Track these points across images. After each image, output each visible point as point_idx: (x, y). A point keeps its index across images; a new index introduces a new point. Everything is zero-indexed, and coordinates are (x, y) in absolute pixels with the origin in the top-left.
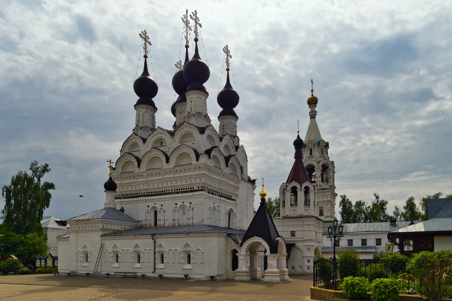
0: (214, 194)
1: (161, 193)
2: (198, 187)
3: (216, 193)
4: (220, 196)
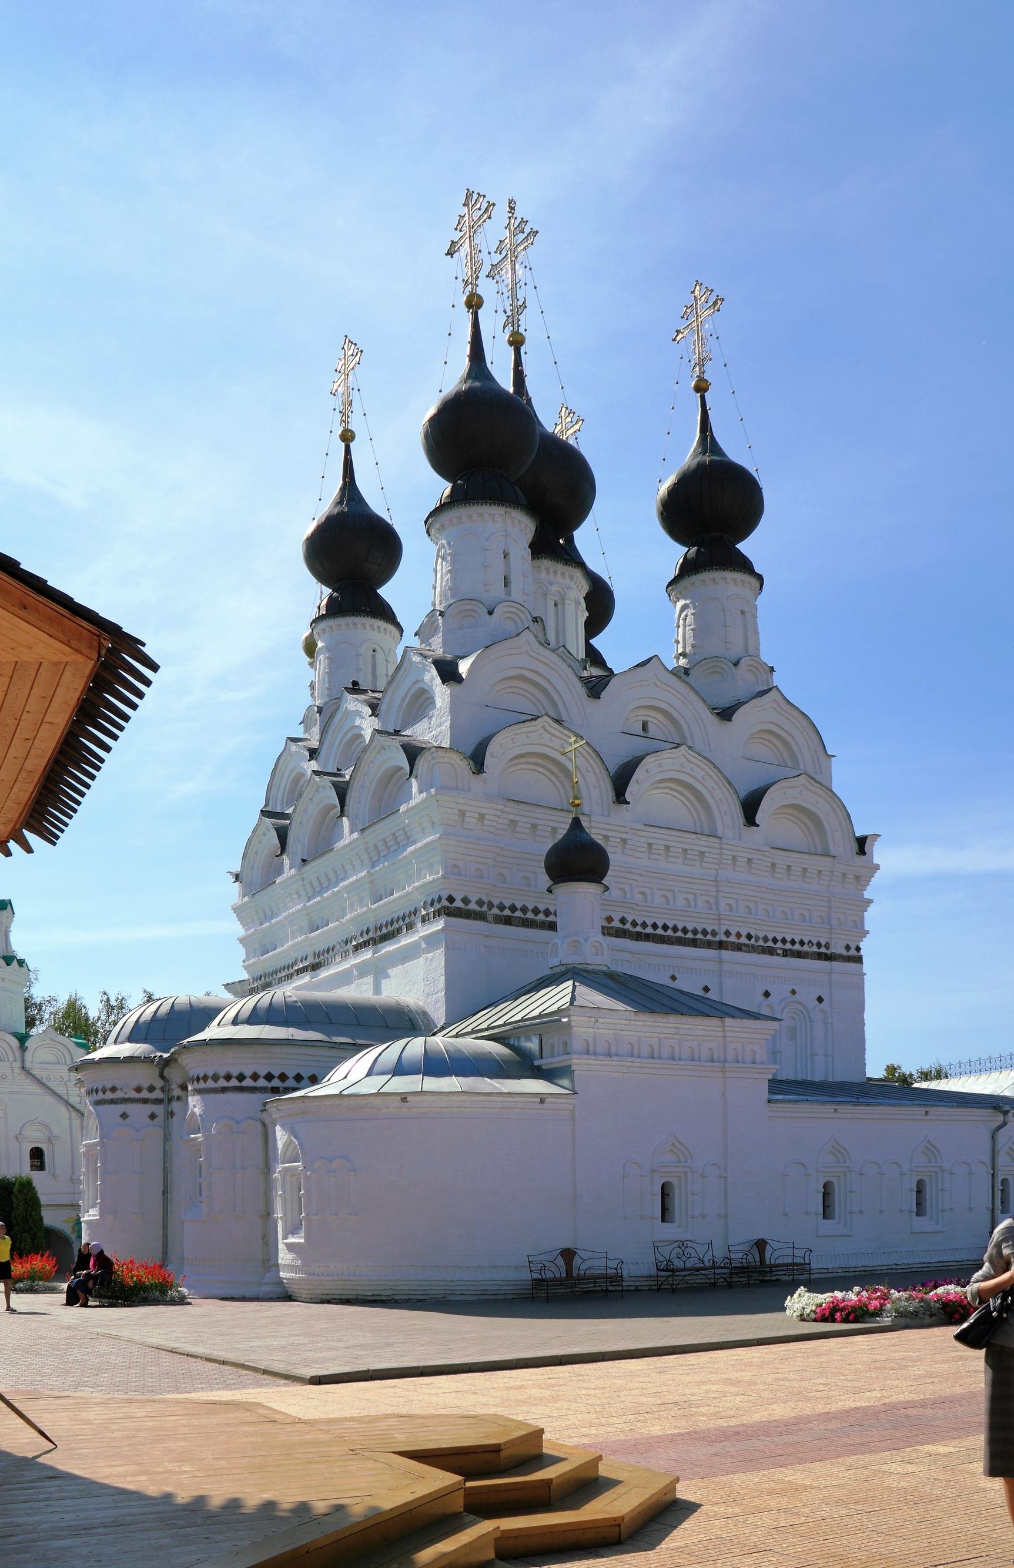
1: (699, 936)
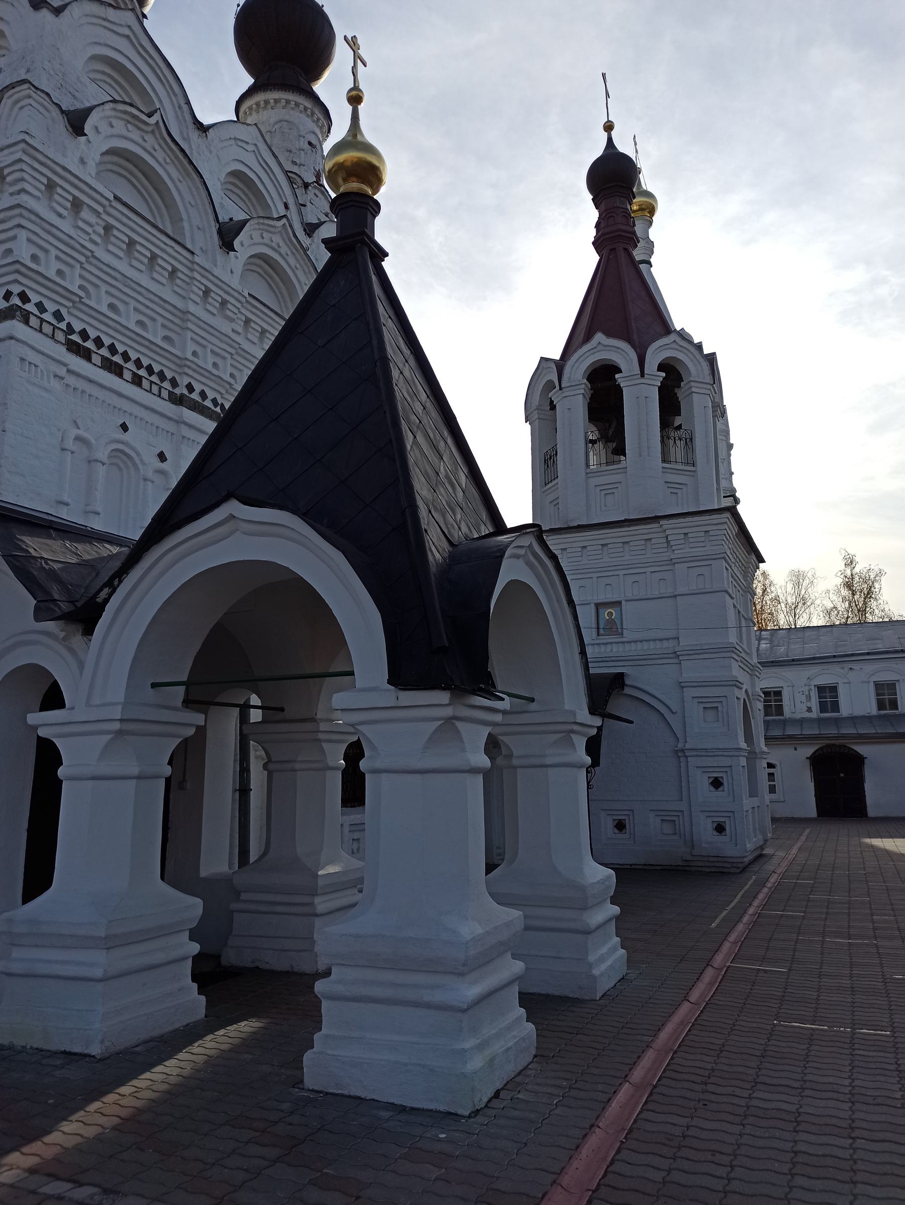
0: (127, 375)
3: (142, 372)
4: (178, 400)
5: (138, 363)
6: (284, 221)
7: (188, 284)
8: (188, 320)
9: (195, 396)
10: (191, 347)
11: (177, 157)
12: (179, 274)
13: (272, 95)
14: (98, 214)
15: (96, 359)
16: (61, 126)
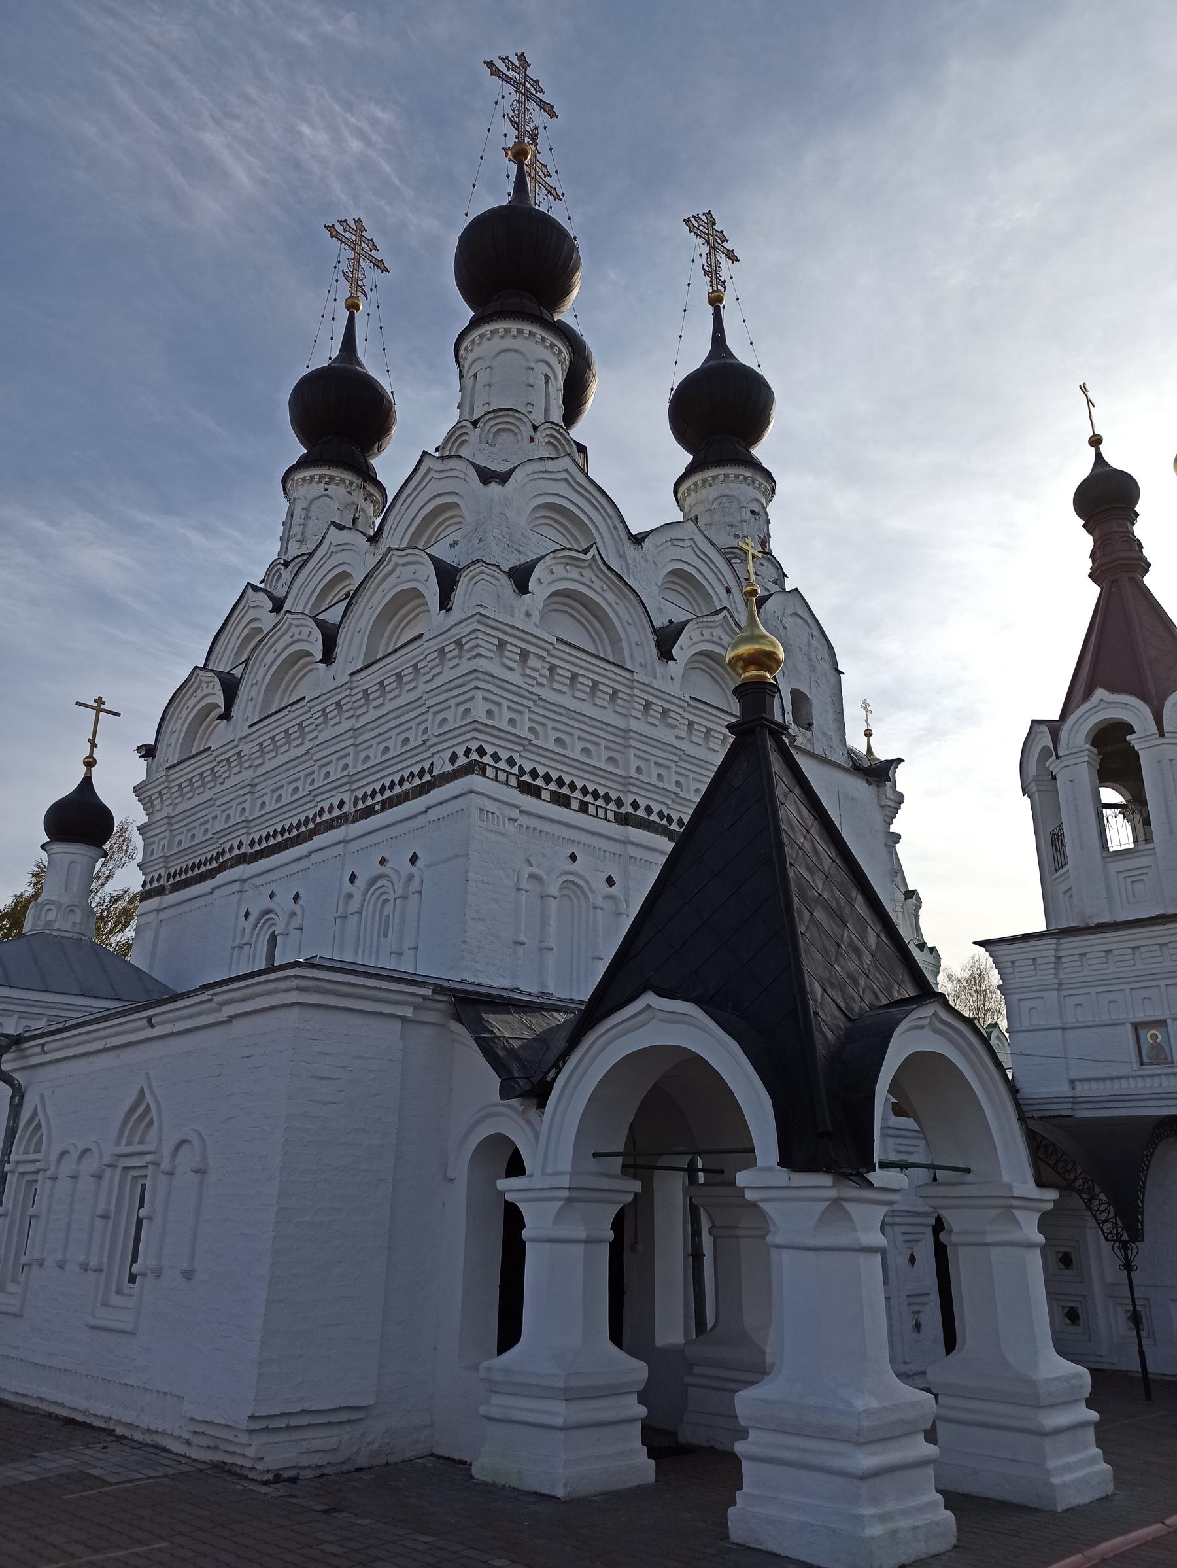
0: (575, 804)
2: (453, 758)
3: (589, 799)
4: (623, 820)
5: (584, 791)
6: (725, 612)
7: (628, 701)
8: (630, 738)
9: (641, 813)
10: (635, 763)
11: (613, 583)
12: (620, 695)
13: (709, 474)
14: (542, 658)
15: (546, 795)
16: (507, 585)
